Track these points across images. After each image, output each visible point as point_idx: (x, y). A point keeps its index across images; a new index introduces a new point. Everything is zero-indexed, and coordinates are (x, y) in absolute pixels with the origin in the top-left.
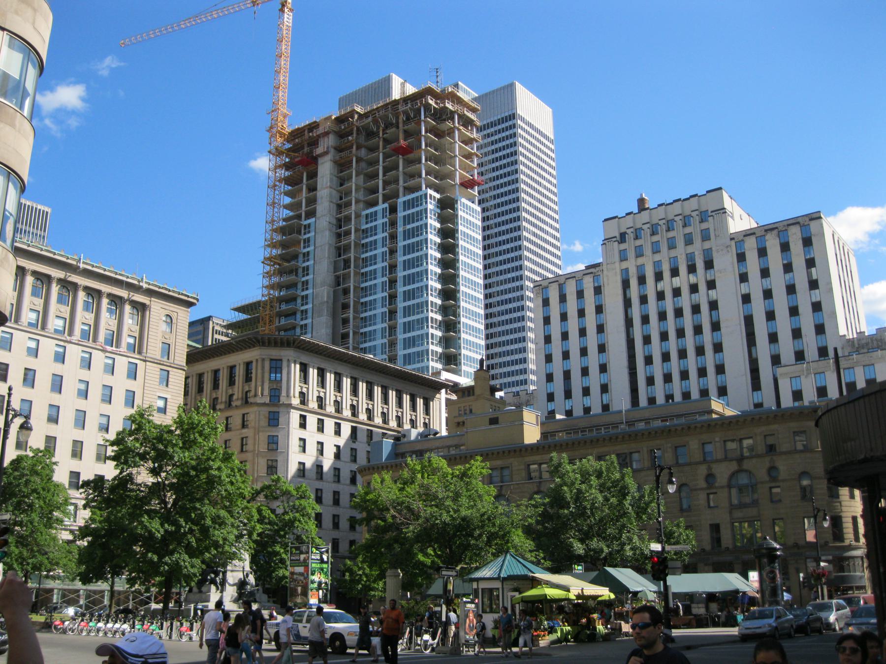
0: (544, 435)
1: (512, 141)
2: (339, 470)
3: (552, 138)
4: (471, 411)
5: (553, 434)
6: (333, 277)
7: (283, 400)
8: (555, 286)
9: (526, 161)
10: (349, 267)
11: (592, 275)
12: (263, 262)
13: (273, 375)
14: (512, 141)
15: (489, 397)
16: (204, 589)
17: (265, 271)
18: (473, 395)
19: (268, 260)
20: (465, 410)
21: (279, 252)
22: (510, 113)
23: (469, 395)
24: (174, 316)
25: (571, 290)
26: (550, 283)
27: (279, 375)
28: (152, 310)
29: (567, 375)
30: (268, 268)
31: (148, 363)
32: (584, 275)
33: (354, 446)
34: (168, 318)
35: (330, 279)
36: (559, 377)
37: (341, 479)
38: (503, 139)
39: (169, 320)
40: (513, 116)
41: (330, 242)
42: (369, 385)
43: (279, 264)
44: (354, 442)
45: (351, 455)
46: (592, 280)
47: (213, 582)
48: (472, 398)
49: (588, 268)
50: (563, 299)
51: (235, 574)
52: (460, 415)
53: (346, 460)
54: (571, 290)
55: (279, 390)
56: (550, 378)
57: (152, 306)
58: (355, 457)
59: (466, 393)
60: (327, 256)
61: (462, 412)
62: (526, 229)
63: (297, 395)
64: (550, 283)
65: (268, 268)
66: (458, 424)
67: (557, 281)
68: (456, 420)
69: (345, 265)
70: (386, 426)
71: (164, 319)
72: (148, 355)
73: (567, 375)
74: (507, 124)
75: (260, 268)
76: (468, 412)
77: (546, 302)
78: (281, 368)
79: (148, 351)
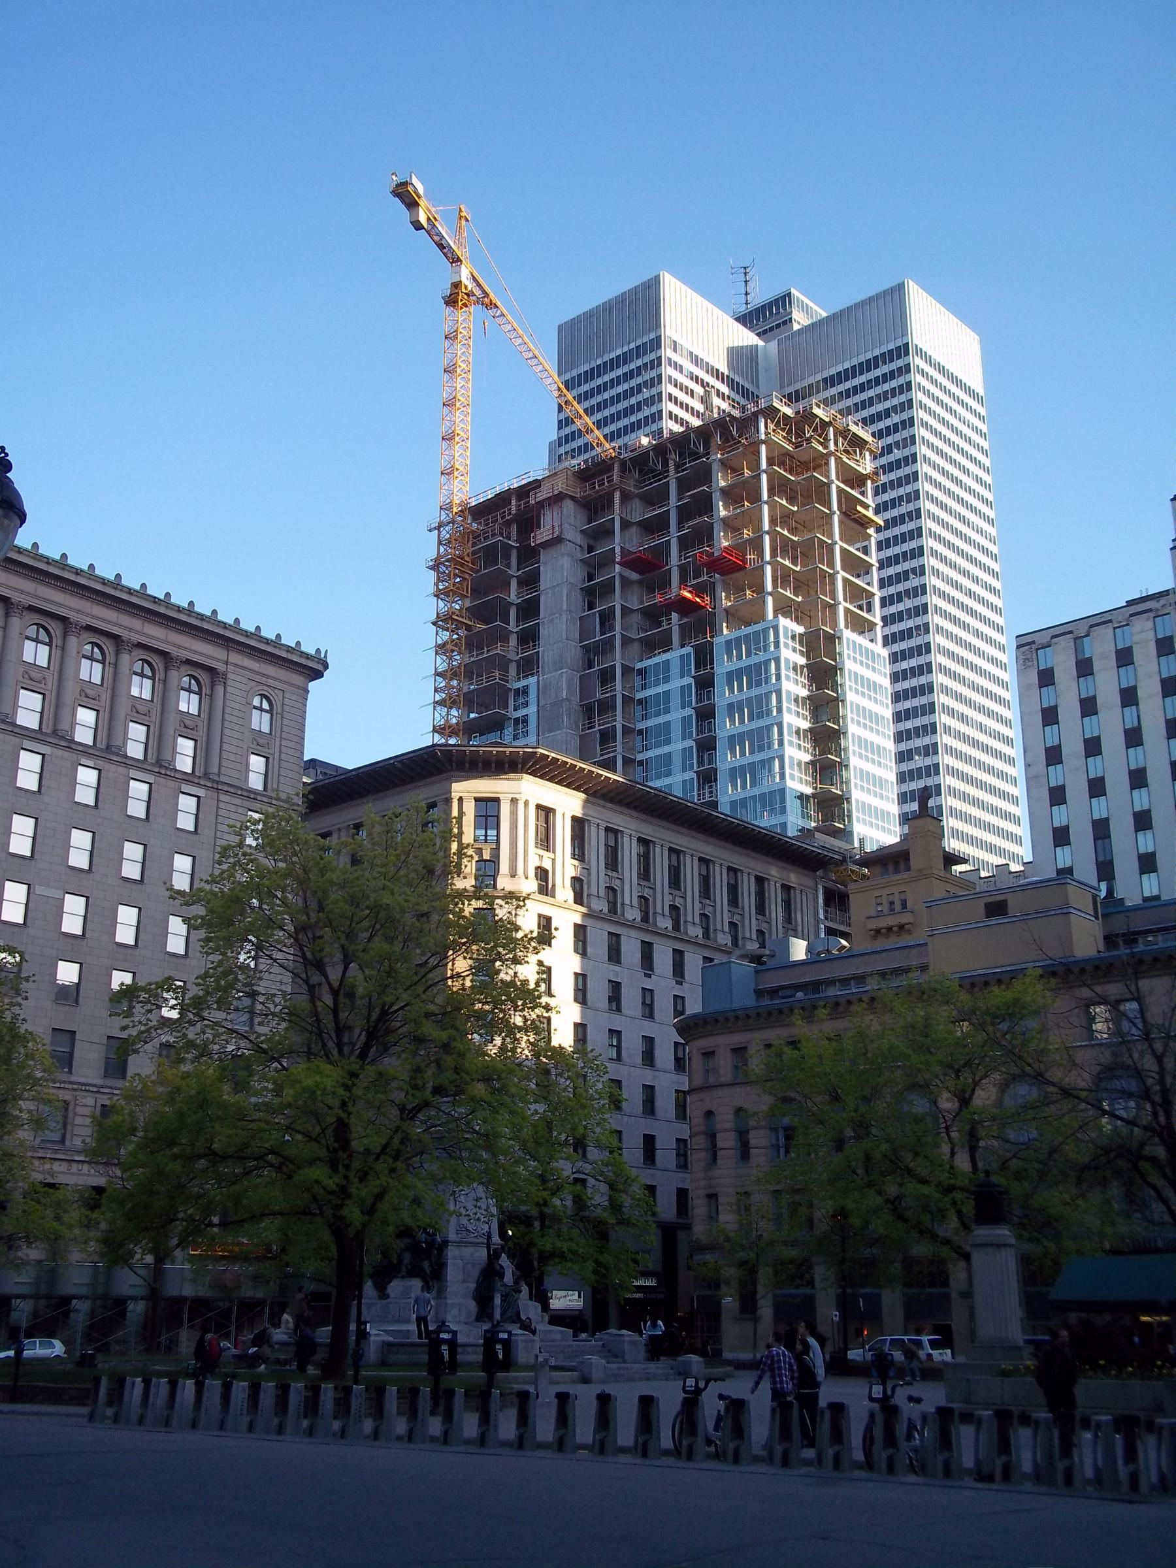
0: (1110, 940)
1: (903, 398)
2: (619, 1033)
3: (982, 393)
4: (904, 904)
5: (1131, 938)
6: (579, 649)
7: (504, 883)
8: (1066, 643)
9: (933, 439)
10: (612, 629)
11: (1151, 615)
12: (434, 624)
13: (482, 832)
14: (903, 398)
15: (942, 874)
16: (395, 1287)
17: (440, 642)
18: (908, 869)
19: (442, 621)
20: (892, 903)
21: (468, 604)
22: (899, 343)
23: (897, 872)
24: (277, 697)
25: (1102, 648)
26: (1053, 637)
27: (492, 833)
28: (229, 682)
29: (1101, 829)
30: (445, 635)
31: (223, 797)
32: (1132, 615)
33: (649, 984)
34: (265, 702)
35: (573, 652)
36: (1082, 835)
37: (624, 1054)
38: (885, 396)
39: (266, 706)
40: (904, 350)
41: (571, 580)
42: (674, 857)
43: (468, 628)
44: (649, 976)
45: (644, 1003)
46: (1150, 624)
47: (414, 1272)
48: (904, 875)
49: (1130, 603)
50: (1085, 668)
51: (468, 1251)
52: (880, 914)
53: (632, 1013)
54: (1102, 648)
55: (495, 860)
56: (1061, 836)
57: (230, 676)
58: (651, 1007)
59: (891, 868)
60: (565, 607)
61: (885, 907)
62: (936, 572)
63: (532, 873)
64: (1053, 637)
65: (445, 635)
66: (878, 931)
67: (1071, 632)
68: (874, 924)
69: (602, 623)
70: (709, 943)
71: (256, 702)
72: (223, 779)
73: (1101, 829)
74: (893, 366)
75: (430, 637)
76: (898, 906)
77: (1046, 678)
78: (498, 817)
79: (223, 770)
